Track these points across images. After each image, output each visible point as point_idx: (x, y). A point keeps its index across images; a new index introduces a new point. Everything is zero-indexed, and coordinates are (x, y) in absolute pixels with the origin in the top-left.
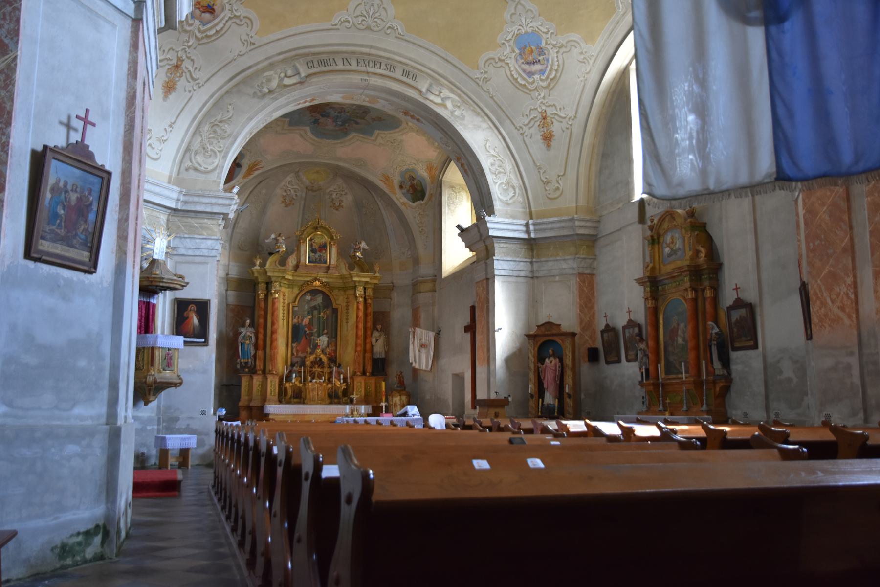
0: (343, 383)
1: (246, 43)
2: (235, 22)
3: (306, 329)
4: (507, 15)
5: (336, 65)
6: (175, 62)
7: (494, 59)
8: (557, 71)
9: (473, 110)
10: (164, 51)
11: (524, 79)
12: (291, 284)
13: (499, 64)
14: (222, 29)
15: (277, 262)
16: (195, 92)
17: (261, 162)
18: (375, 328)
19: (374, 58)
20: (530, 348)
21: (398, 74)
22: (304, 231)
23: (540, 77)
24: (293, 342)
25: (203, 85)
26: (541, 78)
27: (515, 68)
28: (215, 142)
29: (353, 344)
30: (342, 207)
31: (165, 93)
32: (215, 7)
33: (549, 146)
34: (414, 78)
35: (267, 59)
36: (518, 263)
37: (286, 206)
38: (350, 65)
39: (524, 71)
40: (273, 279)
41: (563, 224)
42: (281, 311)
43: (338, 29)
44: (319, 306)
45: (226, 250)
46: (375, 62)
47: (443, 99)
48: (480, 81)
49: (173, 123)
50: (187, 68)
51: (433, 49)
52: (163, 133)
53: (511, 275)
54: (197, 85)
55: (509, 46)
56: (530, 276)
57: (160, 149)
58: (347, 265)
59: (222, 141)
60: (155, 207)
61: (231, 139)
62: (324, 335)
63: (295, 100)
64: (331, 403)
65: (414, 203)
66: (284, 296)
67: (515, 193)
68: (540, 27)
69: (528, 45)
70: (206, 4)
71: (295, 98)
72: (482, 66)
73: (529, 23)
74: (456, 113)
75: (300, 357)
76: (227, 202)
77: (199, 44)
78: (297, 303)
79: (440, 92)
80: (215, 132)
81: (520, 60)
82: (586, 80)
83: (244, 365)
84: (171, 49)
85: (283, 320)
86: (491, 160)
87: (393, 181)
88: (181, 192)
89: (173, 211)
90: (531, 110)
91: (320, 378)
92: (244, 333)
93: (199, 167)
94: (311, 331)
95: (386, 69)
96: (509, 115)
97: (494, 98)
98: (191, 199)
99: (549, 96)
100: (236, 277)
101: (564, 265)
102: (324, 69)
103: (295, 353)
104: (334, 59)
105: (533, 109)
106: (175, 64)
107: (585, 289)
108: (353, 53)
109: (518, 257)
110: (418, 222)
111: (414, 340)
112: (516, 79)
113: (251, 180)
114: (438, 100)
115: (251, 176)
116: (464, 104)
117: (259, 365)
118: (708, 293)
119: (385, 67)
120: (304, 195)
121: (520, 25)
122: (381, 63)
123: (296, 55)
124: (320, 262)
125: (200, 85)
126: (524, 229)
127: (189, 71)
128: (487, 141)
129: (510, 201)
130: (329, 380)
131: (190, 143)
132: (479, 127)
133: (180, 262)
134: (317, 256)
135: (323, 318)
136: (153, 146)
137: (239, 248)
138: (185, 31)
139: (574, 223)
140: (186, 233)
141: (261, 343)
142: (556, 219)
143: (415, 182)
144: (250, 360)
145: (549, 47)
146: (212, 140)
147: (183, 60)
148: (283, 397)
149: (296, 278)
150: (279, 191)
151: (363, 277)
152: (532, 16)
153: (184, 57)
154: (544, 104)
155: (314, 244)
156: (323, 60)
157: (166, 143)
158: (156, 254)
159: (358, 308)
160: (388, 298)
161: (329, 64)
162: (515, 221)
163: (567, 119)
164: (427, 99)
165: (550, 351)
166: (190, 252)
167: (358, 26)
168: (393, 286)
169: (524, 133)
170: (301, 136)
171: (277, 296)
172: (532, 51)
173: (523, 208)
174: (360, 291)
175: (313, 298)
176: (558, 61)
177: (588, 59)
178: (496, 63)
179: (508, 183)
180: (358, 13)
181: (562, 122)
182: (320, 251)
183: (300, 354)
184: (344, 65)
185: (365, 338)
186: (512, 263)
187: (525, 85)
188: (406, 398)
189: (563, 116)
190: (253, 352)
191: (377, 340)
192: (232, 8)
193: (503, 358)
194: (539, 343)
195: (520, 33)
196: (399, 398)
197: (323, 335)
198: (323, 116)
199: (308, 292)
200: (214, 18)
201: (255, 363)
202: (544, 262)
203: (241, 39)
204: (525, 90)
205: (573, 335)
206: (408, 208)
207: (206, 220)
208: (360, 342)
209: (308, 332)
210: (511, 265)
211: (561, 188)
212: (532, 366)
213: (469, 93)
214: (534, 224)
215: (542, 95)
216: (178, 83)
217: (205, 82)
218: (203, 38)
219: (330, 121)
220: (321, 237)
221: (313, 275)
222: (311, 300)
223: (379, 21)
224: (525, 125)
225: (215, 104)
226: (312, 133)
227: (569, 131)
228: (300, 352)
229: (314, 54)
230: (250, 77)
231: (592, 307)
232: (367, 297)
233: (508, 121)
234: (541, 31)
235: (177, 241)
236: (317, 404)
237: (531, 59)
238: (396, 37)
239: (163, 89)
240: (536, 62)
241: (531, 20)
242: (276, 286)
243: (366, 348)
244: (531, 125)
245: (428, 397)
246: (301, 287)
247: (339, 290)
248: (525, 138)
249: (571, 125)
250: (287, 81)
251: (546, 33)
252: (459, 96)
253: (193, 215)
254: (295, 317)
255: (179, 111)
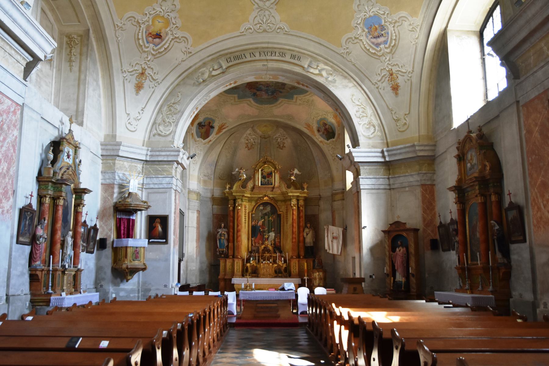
0: (284, 264)
1: (185, 53)
2: (176, 41)
3: (260, 228)
4: (355, 7)
5: (246, 58)
6: (140, 71)
7: (351, 38)
8: (395, 40)
9: (342, 75)
10: (133, 66)
11: (373, 49)
12: (250, 200)
13: (356, 41)
14: (168, 47)
15: (241, 186)
16: (156, 88)
17: (225, 123)
18: (306, 226)
19: (270, 50)
20: (386, 240)
21: (288, 58)
22: (257, 165)
23: (385, 46)
24: (252, 237)
25: (161, 83)
26: (386, 46)
27: (367, 42)
28: (170, 116)
29: (291, 237)
30: (285, 147)
31: (137, 90)
32: (161, 34)
33: (397, 94)
34: (299, 59)
35: (201, 61)
36: (378, 179)
37: (249, 150)
38: (255, 56)
39: (373, 43)
40: (237, 197)
41: (407, 150)
42: (243, 217)
43: (245, 35)
44: (269, 213)
45: (212, 180)
46: (272, 52)
47: (319, 71)
48: (344, 54)
49: (144, 108)
50: (149, 74)
51: (310, 38)
52: (138, 115)
53: (373, 188)
54: (157, 83)
55: (360, 28)
56: (388, 187)
57: (136, 124)
58: (286, 185)
59: (174, 116)
60: (133, 160)
61: (180, 114)
63: (222, 84)
64: (276, 277)
65: (328, 140)
66: (245, 207)
67: (375, 130)
68: (379, 11)
69: (373, 25)
70: (155, 33)
71: (222, 83)
72: (344, 44)
73: (371, 10)
74: (329, 79)
75: (257, 246)
76: (176, 153)
77: (154, 58)
78: (254, 212)
79: (318, 66)
80: (170, 110)
81: (369, 36)
82: (417, 43)
83: (221, 253)
84: (137, 64)
85: (245, 223)
86: (356, 108)
87: (313, 128)
88: (148, 150)
89: (145, 162)
90: (382, 70)
91: (269, 260)
92: (220, 233)
93: (161, 133)
95: (279, 56)
96: (367, 75)
97: (355, 64)
98: (154, 153)
99: (393, 58)
100: (218, 196)
101: (411, 179)
102: (237, 61)
103: (254, 244)
104: (244, 54)
105: (383, 69)
106: (141, 72)
107: (427, 196)
108: (257, 48)
109: (378, 175)
110: (331, 153)
111: (328, 234)
112: (369, 50)
113: (220, 136)
114: (317, 72)
115: (221, 133)
116: (335, 72)
117: (230, 252)
118: (493, 198)
119: (279, 55)
120: (259, 141)
121: (365, 12)
122: (275, 52)
123: (220, 55)
124: (268, 184)
125: (159, 83)
126: (381, 155)
127: (151, 75)
128: (353, 95)
129: (371, 136)
130: (275, 262)
131: (156, 119)
132: (347, 86)
133: (151, 193)
134: (266, 181)
136: (131, 124)
137: (220, 178)
138: (145, 52)
139: (415, 148)
140: (154, 175)
141: (231, 238)
142: (402, 146)
143: (327, 127)
144: (224, 249)
145: (387, 24)
146: (168, 115)
147: (146, 69)
148: (244, 273)
149: (252, 196)
150: (243, 140)
151: (295, 193)
152: (372, 4)
153: (146, 67)
154: (390, 64)
155: (264, 173)
156: (237, 56)
157: (140, 121)
158: (131, 189)
159: (293, 214)
160: (317, 206)
161: (241, 58)
162: (373, 150)
163: (407, 73)
164: (308, 72)
165: (399, 242)
166: (156, 186)
167: (258, 31)
168: (320, 197)
169: (379, 86)
170: (248, 104)
171: (240, 208)
172: (376, 29)
173: (382, 140)
174: (294, 202)
176: (395, 33)
177: (416, 28)
178: (353, 40)
179: (370, 123)
180: (256, 22)
181: (403, 76)
182: (268, 177)
183: (257, 245)
184: (251, 57)
185: (299, 233)
186: (373, 180)
187: (375, 53)
188: (323, 273)
189: (404, 71)
190: (226, 244)
191: (307, 234)
192: (173, 33)
193: (368, 248)
194: (391, 238)
195: (366, 18)
196: (318, 273)
197: (271, 232)
198: (258, 90)
199: (261, 204)
200: (162, 41)
201: (228, 251)
202: (397, 178)
203: (182, 51)
204: (375, 57)
205: (416, 230)
206: (324, 144)
207: (165, 166)
208: (296, 236)
209: (262, 230)
210: (373, 181)
211: (407, 123)
212: (387, 253)
213: (338, 64)
214: (387, 151)
215: (388, 58)
216: (144, 84)
217: (163, 80)
218: (157, 54)
219: (263, 93)
220: (268, 168)
221: (263, 193)
222: (263, 209)
223: (271, 25)
224: (379, 81)
225: (170, 93)
226: (255, 102)
227: (410, 81)
228: (257, 243)
229: (231, 53)
230: (191, 73)
231: (433, 209)
232: (299, 206)
233: (367, 80)
234: (380, 13)
235: (148, 180)
236: (267, 277)
237: (376, 34)
238: (284, 34)
239: (134, 88)
240: (381, 36)
241: (371, 7)
242: (239, 201)
243: (300, 241)
244: (382, 81)
245: (341, 273)
246: (256, 201)
247: (282, 202)
248: (380, 90)
249: (411, 77)
250: (214, 73)
251: (384, 14)
252: (331, 67)
253: (157, 163)
255: (147, 100)
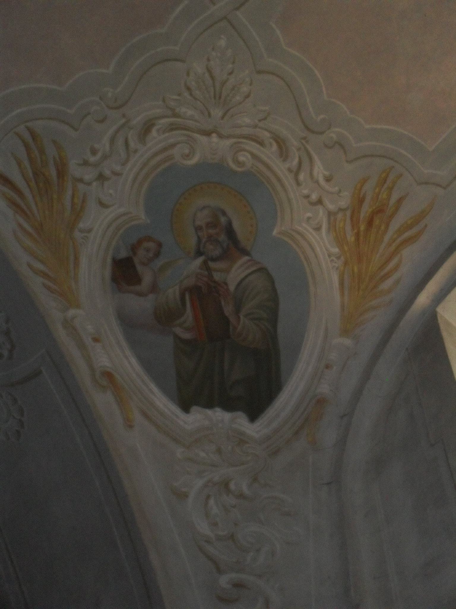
65: (186, 409)
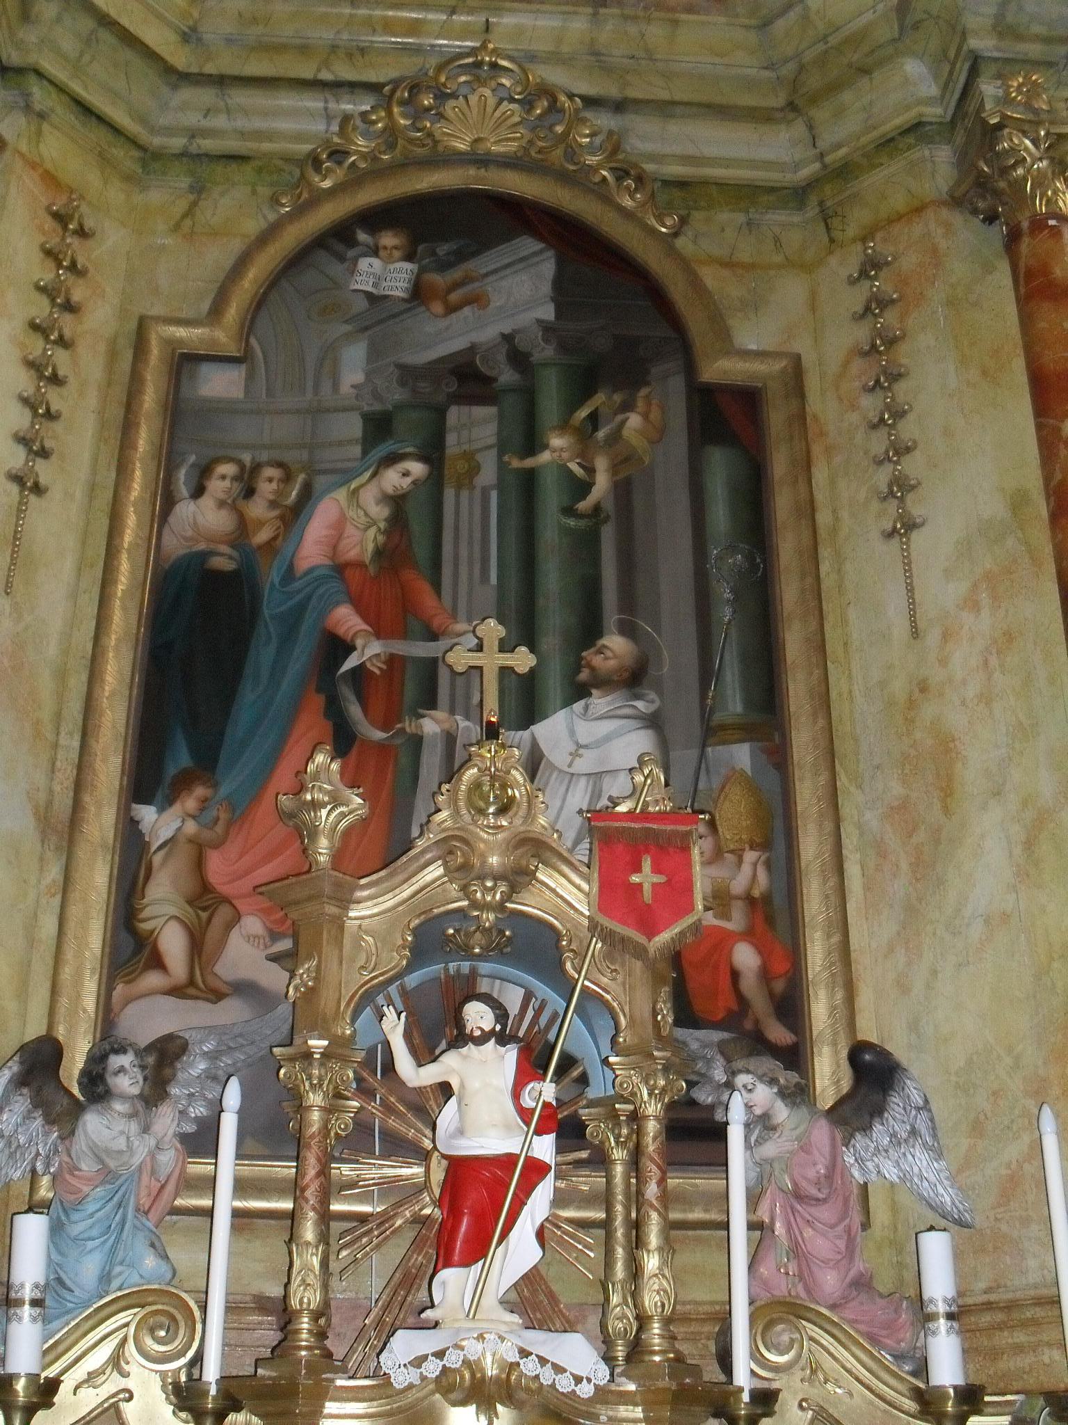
3: (346, 619)
44: (519, 358)
62: (600, 702)
94: (421, 649)
103: (173, 943)
135: (583, 488)
175: (437, 279)
197: (579, 692)
222: (418, 293)
228: (252, 924)
254: (204, 473)
